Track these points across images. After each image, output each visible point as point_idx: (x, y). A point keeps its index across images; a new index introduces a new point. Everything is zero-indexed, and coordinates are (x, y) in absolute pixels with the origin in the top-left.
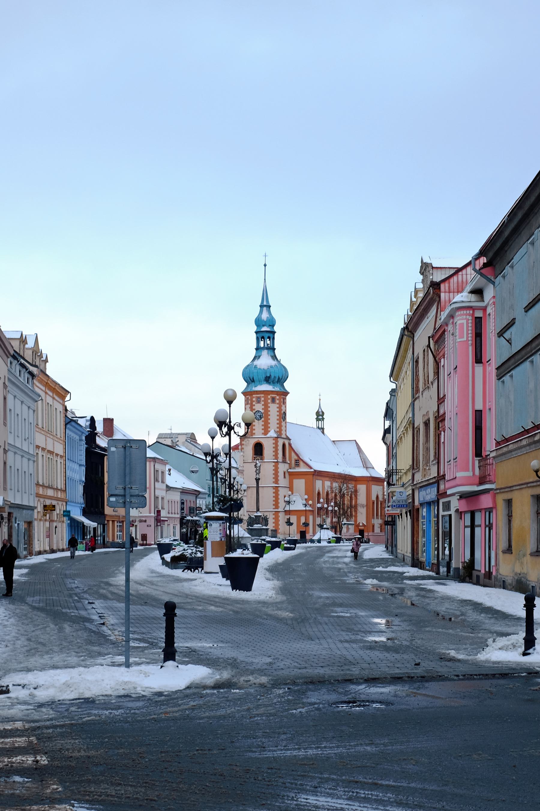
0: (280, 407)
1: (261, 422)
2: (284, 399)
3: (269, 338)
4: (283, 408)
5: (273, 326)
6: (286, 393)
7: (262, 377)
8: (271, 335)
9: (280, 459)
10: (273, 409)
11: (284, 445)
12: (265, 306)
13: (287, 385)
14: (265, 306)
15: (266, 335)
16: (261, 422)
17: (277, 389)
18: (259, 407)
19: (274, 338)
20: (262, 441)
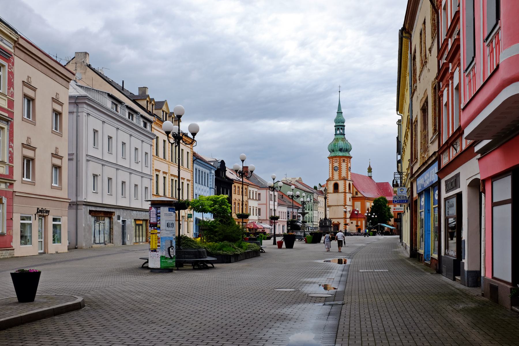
0: (347, 165)
1: (337, 172)
3: (342, 129)
4: (349, 165)
5: (344, 123)
6: (350, 157)
7: (338, 149)
8: (343, 128)
9: (347, 190)
10: (344, 165)
11: (350, 184)
12: (340, 113)
13: (351, 153)
14: (340, 113)
15: (340, 127)
16: (337, 172)
17: (347, 155)
18: (336, 164)
20: (338, 182)
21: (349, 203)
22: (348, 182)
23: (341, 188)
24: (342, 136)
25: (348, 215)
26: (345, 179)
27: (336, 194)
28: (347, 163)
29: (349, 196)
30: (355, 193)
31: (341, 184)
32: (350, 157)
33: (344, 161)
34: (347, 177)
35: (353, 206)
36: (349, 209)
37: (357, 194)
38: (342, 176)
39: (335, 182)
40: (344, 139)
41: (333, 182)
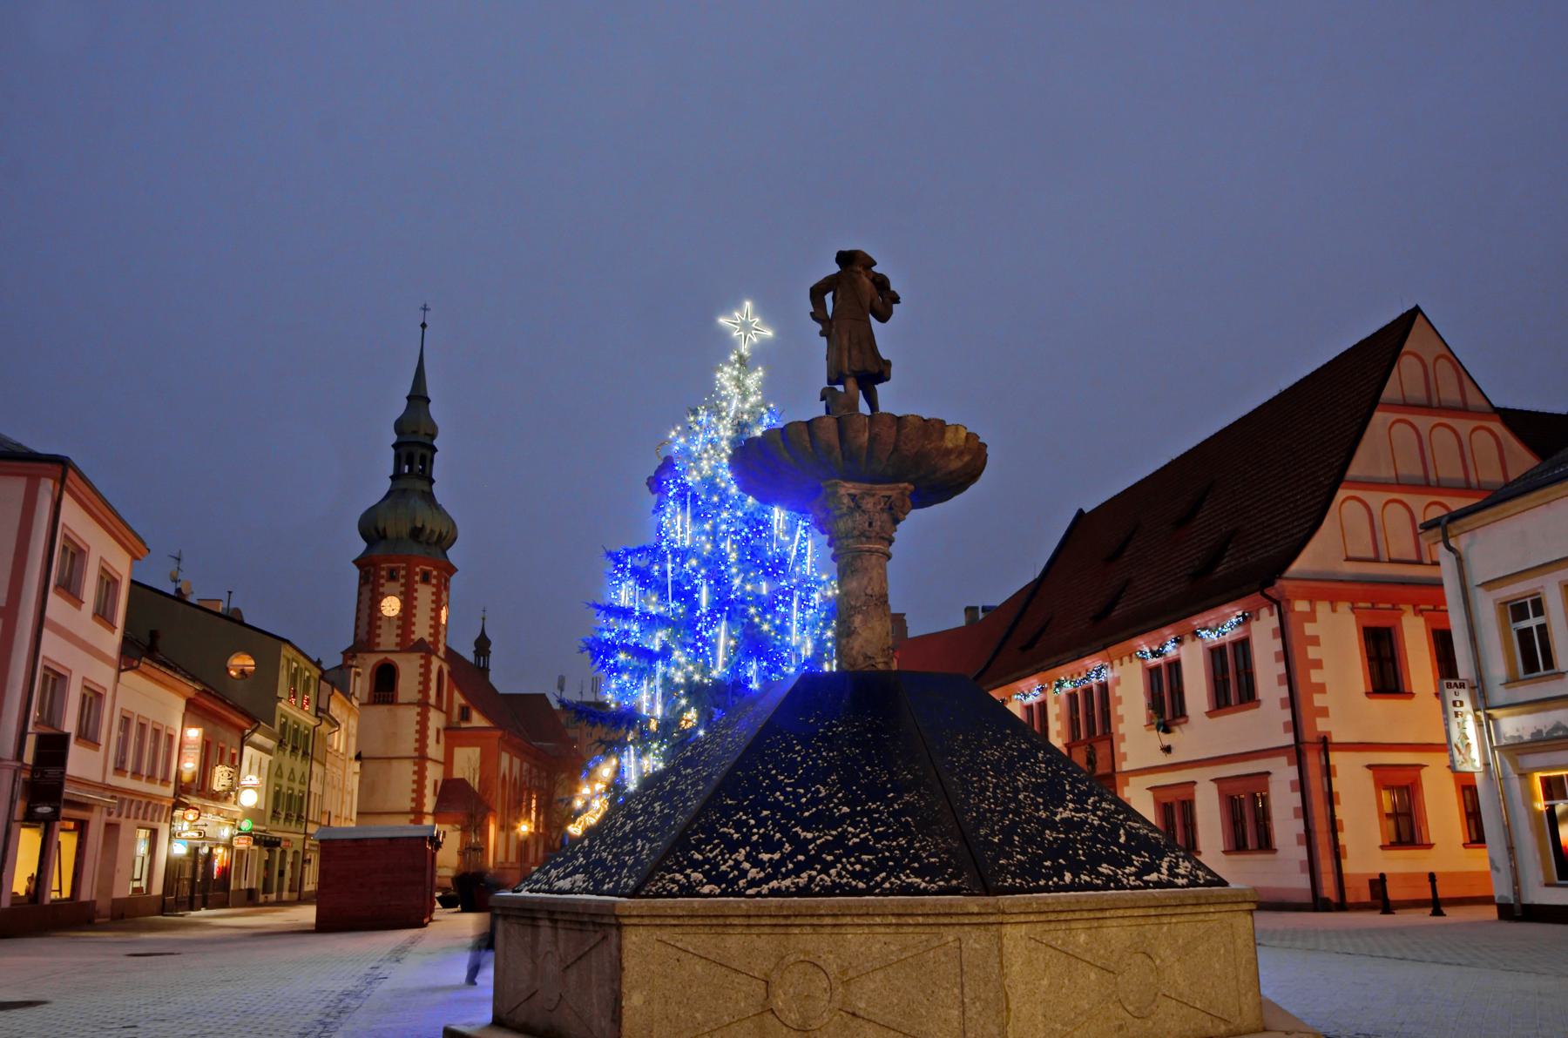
2: (447, 580)
5: (433, 437)
8: (429, 454)
9: (432, 700)
12: (418, 398)
13: (453, 554)
14: (418, 398)
15: (419, 451)
19: (432, 461)
20: (391, 657)
21: (434, 750)
22: (435, 664)
23: (408, 685)
24: (421, 485)
25: (429, 804)
26: (425, 649)
27: (382, 710)
28: (437, 586)
29: (436, 720)
30: (456, 711)
31: (409, 670)
32: (451, 570)
33: (426, 579)
34: (436, 642)
35: (448, 762)
36: (434, 773)
37: (465, 715)
38: (416, 637)
39: (381, 657)
40: (429, 497)
41: (373, 659)
